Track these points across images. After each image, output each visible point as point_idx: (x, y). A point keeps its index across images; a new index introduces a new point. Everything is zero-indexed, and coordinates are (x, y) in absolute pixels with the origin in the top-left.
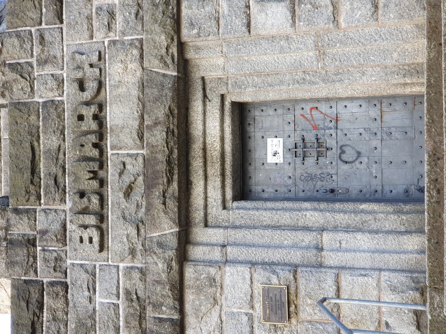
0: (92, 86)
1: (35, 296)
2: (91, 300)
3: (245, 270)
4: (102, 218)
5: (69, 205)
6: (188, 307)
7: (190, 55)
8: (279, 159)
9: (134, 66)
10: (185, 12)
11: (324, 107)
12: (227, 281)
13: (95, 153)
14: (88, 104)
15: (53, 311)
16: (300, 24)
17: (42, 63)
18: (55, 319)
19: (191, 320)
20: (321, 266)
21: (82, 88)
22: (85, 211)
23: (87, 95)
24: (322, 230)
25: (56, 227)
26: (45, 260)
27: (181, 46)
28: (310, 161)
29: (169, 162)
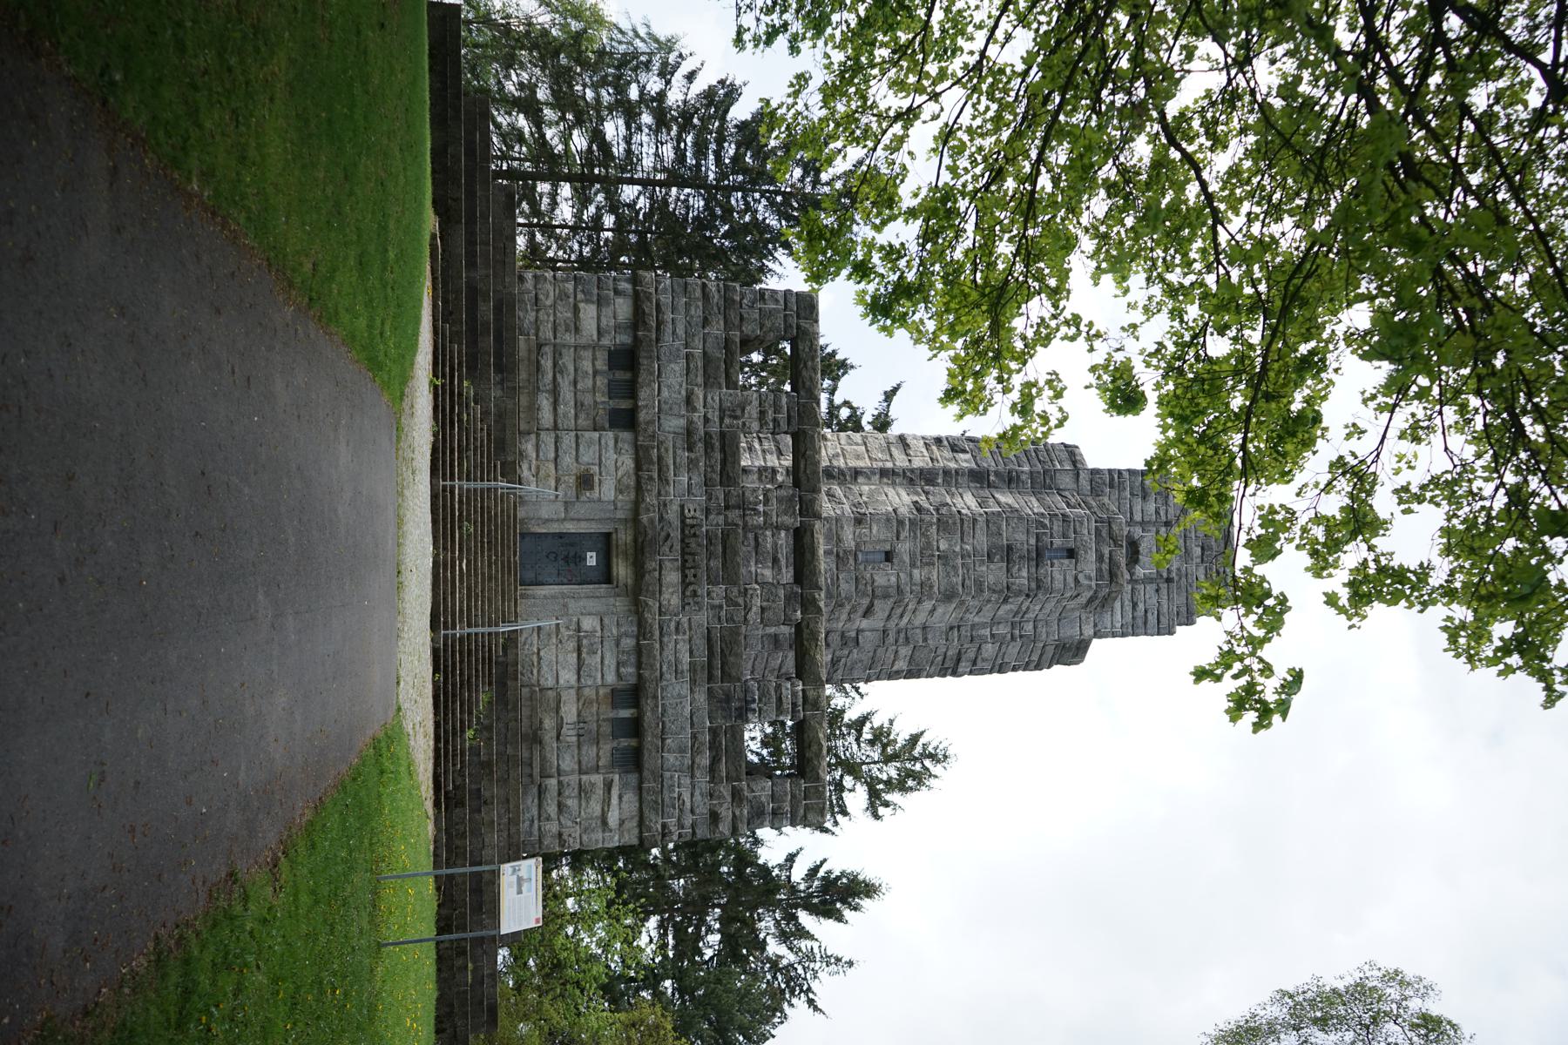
0: (688, 593)
1: (725, 477)
2: (690, 479)
3: (604, 498)
4: (683, 522)
5: (704, 529)
6: (633, 478)
7: (633, 608)
8: (589, 554)
9: (665, 603)
10: (635, 629)
11: (565, 581)
12: (613, 492)
13: (686, 557)
14: (691, 584)
15: (713, 471)
16: (575, 619)
17: (721, 607)
18: (712, 467)
19: (631, 471)
20: (566, 502)
21: (695, 591)
22: (693, 526)
23: (691, 588)
24: (565, 519)
25: (711, 517)
26: (717, 499)
27: (637, 612)
28: (572, 554)
29: (643, 553)
